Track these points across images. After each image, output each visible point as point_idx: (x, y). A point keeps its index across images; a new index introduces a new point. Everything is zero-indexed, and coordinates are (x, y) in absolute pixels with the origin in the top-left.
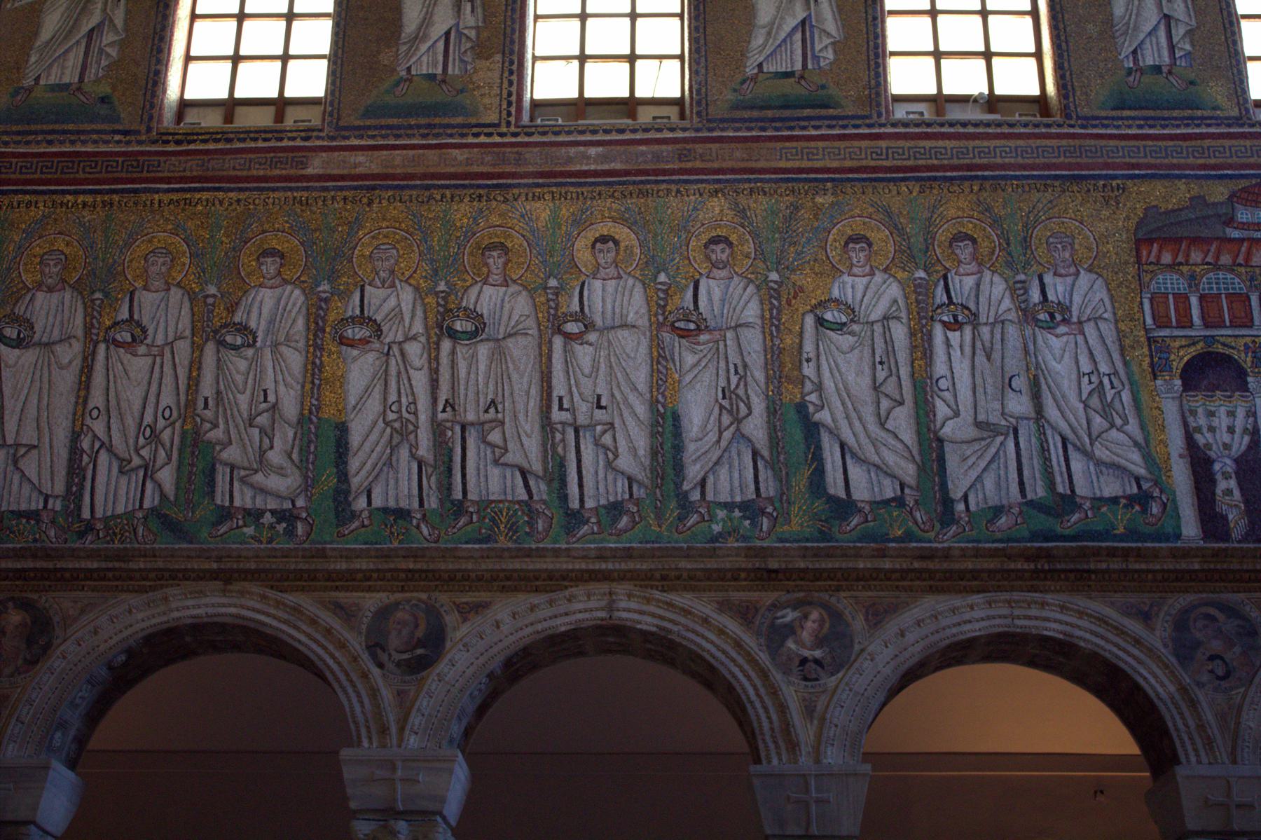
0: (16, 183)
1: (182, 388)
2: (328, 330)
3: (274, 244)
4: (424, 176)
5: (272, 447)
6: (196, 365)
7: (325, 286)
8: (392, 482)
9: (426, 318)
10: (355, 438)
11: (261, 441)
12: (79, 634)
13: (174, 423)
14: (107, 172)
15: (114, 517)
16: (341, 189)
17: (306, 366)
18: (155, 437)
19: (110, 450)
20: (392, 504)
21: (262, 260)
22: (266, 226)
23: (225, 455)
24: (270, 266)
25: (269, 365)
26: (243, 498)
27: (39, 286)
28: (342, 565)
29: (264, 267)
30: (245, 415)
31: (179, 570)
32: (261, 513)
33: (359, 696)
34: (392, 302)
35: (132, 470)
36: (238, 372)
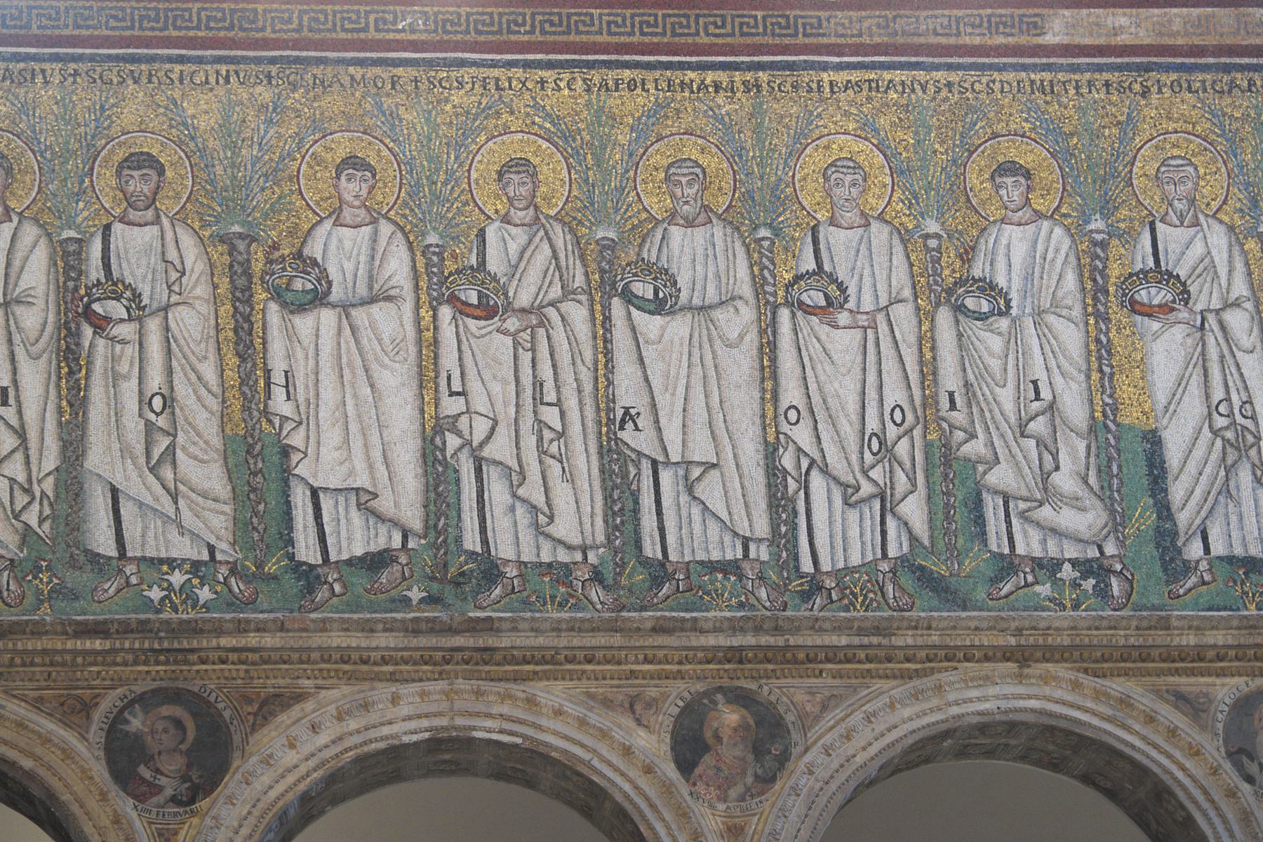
0: (605, 49)
1: (914, 377)
2: (1112, 289)
3: (1012, 154)
4: (1220, 50)
5: (1057, 468)
6: (927, 341)
7: (1097, 224)
8: (1234, 519)
9: (1250, 274)
10: (1173, 455)
11: (1040, 459)
12: (827, 739)
13: (911, 430)
14: (743, 34)
15: (849, 570)
16: (1100, 68)
17: (1087, 345)
18: (886, 451)
19: (825, 471)
20: (1238, 551)
21: (998, 180)
22: (999, 128)
23: (993, 478)
24: (1012, 190)
25: (1035, 342)
26: (1029, 543)
27: (672, 217)
28: (1191, 639)
29: (1003, 192)
30: (1013, 420)
31: (957, 647)
32: (1056, 565)
33: (1225, 821)
34: (1198, 249)
35: (863, 501)
36: (991, 354)
